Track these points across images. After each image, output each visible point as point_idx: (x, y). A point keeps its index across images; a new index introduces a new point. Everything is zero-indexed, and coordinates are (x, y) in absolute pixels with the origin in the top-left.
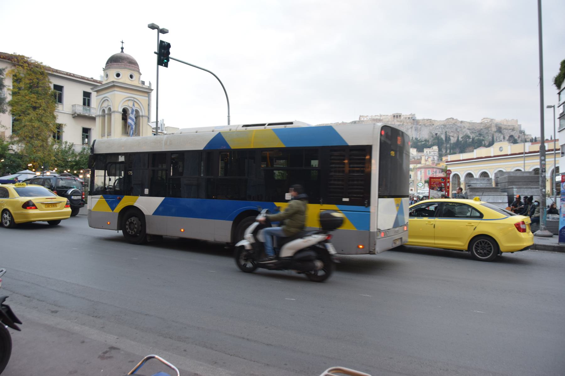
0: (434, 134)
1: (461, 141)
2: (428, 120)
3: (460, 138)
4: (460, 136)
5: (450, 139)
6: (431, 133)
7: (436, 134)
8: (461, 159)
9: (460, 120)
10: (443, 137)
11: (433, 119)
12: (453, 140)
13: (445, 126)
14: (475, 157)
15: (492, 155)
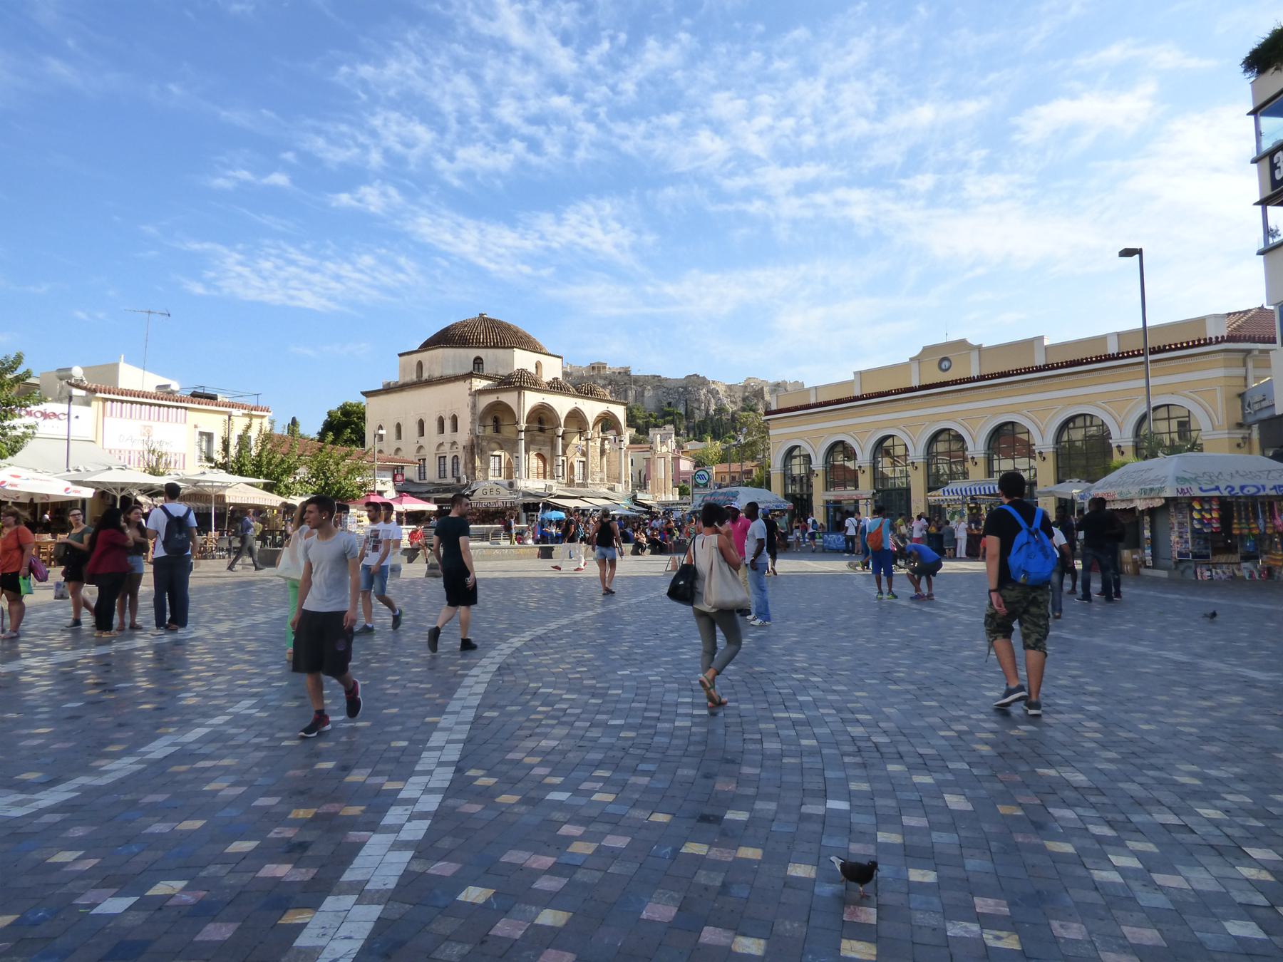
0: (665, 403)
1: (712, 419)
2: (654, 377)
3: (712, 412)
4: (713, 407)
5: (693, 412)
6: (659, 401)
7: (669, 404)
8: (813, 401)
9: (708, 378)
10: (681, 410)
11: (663, 376)
12: (698, 416)
13: (685, 388)
14: (857, 393)
15: (915, 383)
